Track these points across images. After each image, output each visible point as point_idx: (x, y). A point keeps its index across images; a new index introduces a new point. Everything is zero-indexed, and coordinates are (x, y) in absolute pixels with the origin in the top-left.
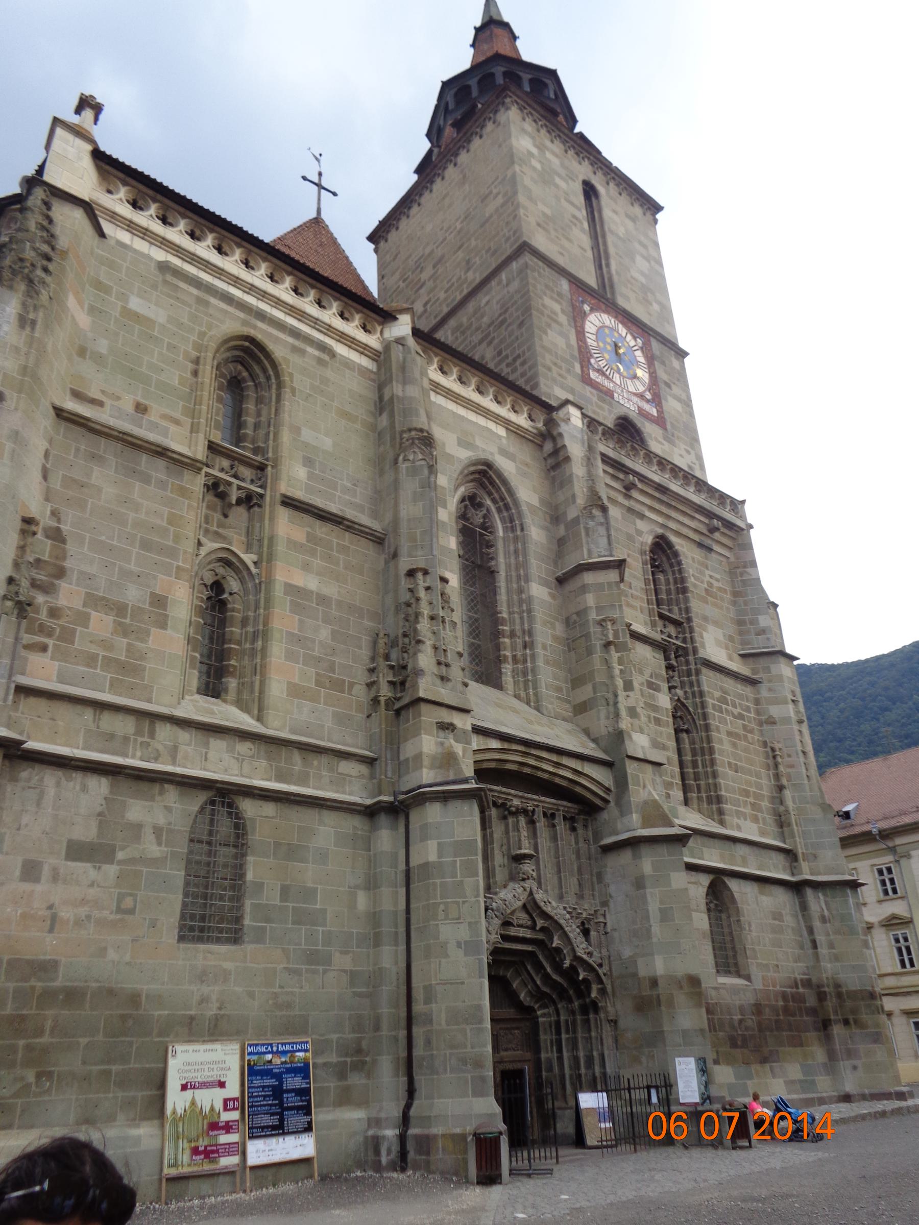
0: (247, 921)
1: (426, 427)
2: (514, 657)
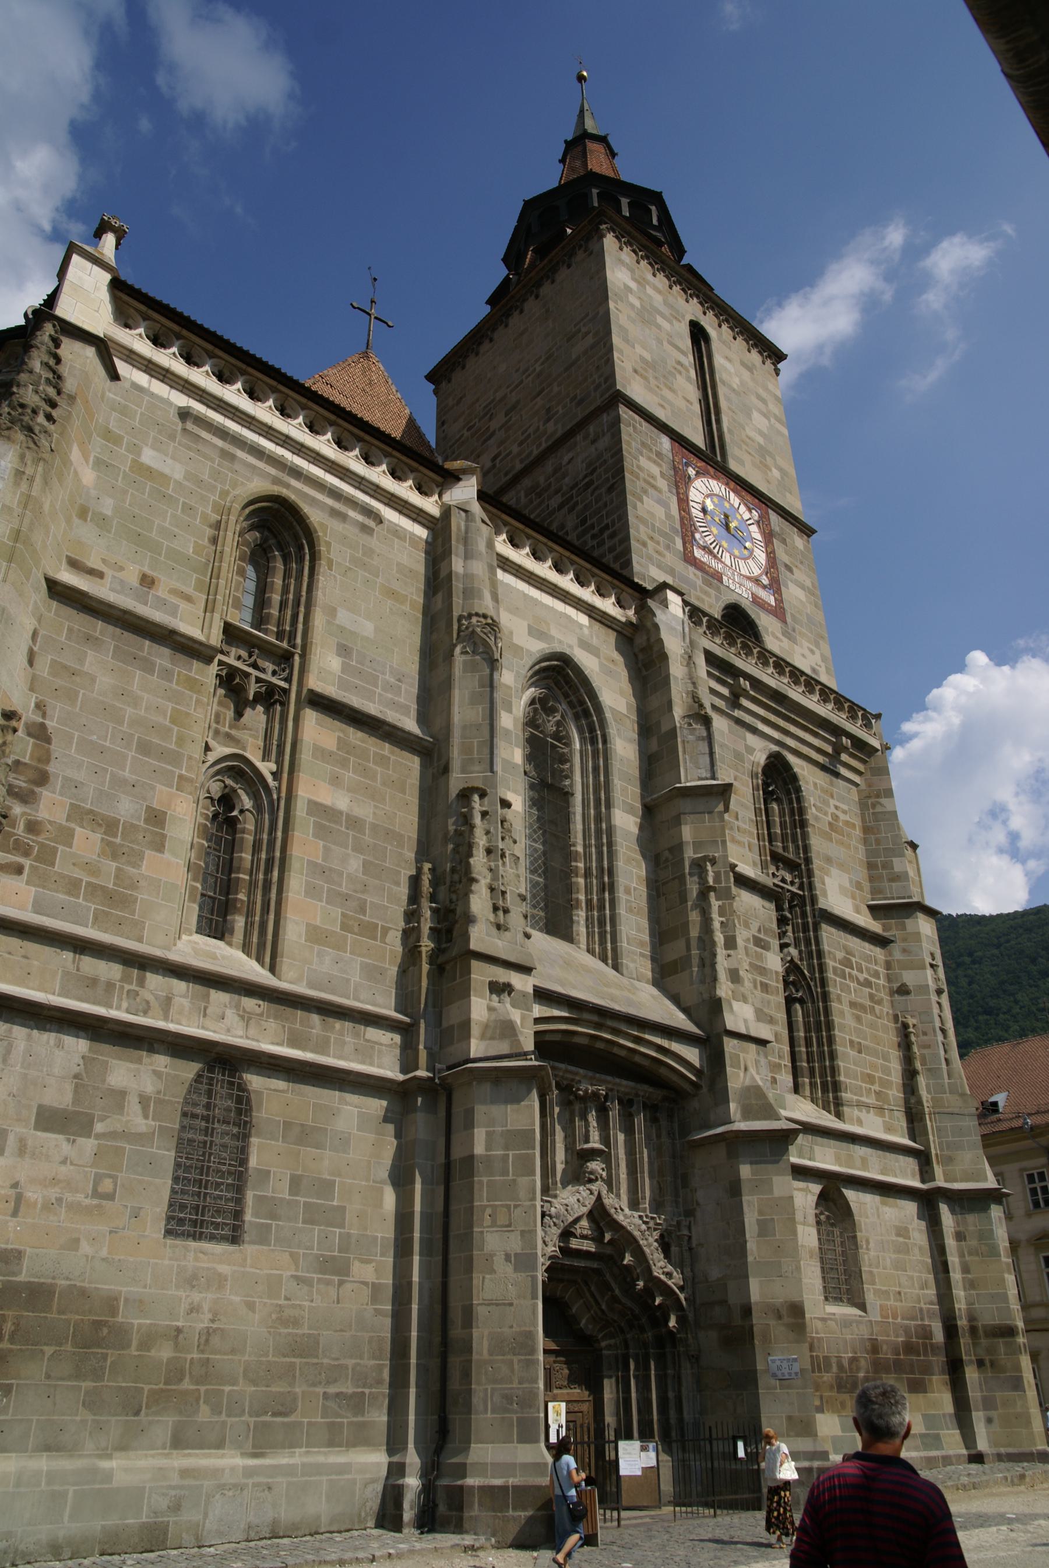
0: (248, 1217)
1: (491, 612)
2: (589, 902)
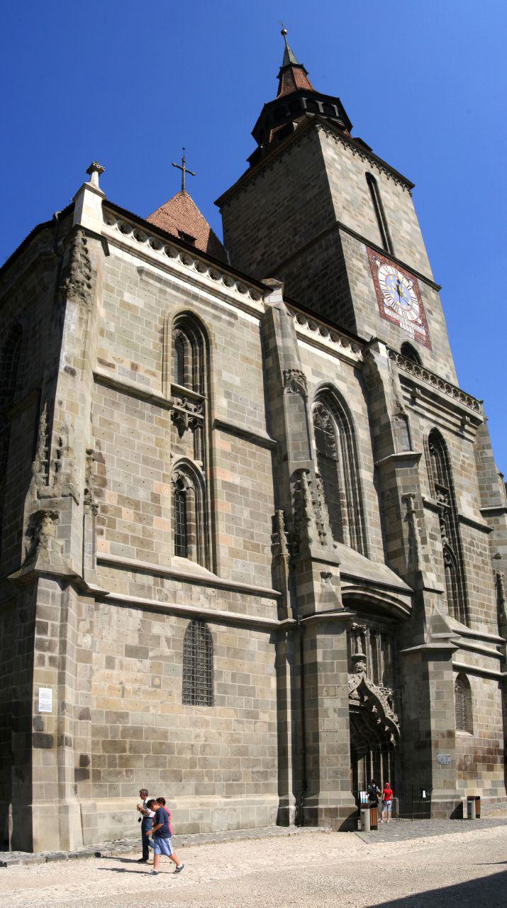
2: (350, 521)
